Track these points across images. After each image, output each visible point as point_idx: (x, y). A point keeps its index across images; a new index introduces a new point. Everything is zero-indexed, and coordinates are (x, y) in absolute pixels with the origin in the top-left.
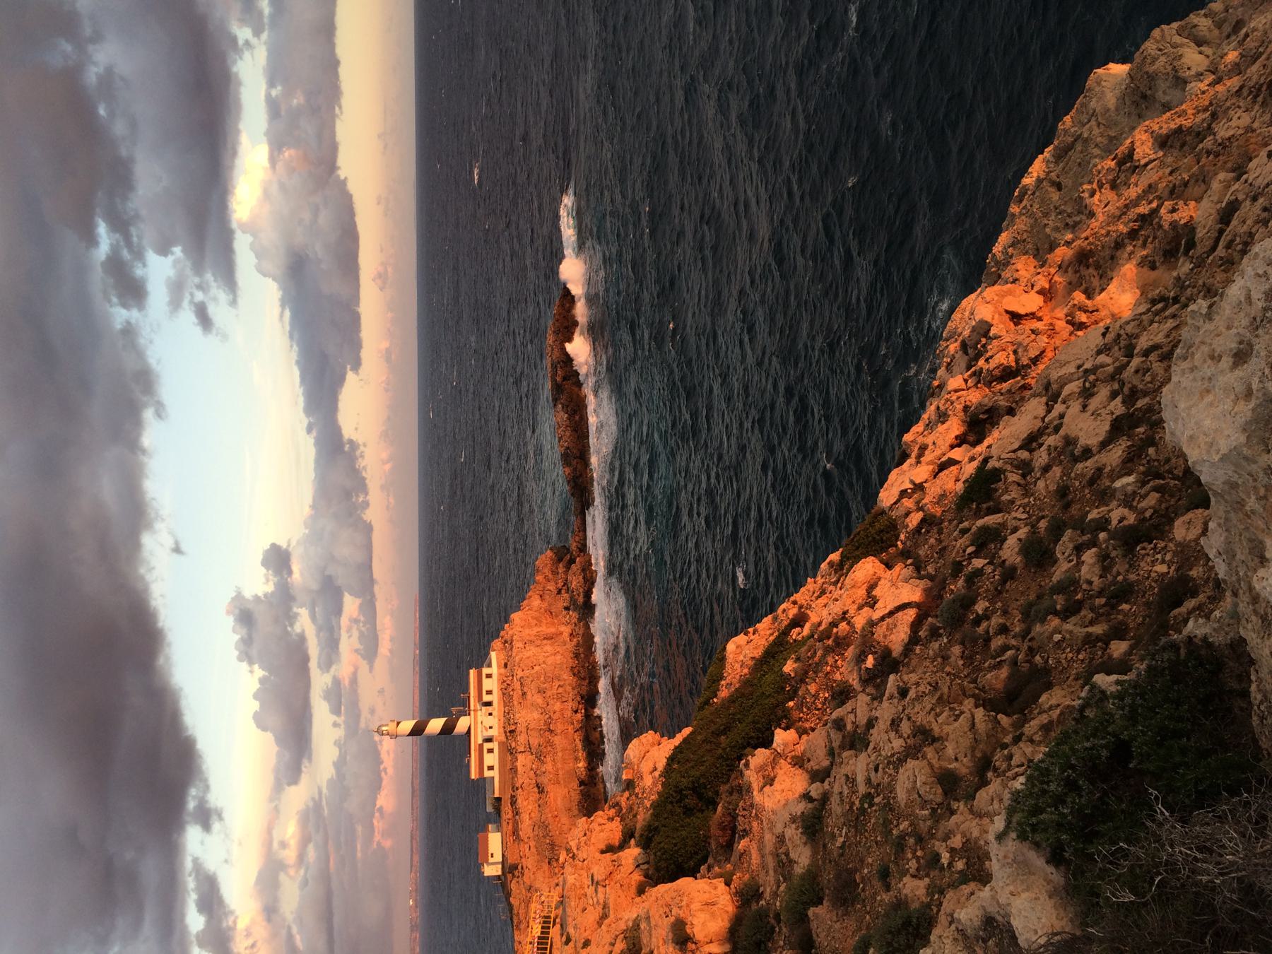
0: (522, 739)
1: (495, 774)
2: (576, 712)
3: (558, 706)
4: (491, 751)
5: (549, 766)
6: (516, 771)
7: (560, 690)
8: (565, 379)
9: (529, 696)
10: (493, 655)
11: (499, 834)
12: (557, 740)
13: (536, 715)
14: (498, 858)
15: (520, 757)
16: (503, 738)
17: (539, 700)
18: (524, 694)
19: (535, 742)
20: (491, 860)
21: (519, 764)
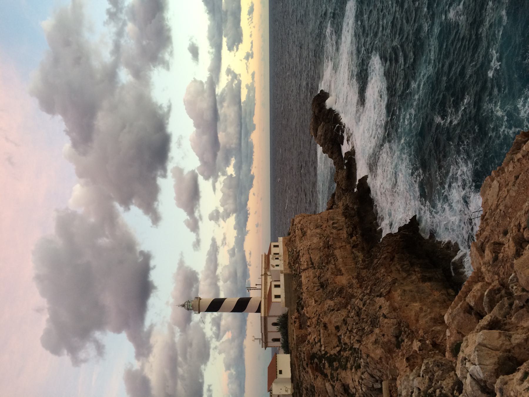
0: (304, 260)
1: (282, 299)
2: (351, 238)
3: (334, 231)
4: (277, 286)
5: (331, 266)
6: (300, 285)
7: (335, 225)
8: (320, 111)
9: (309, 232)
10: (281, 239)
11: (288, 356)
12: (337, 252)
13: (315, 240)
14: (287, 374)
15: (303, 275)
16: (288, 271)
17: (318, 231)
18: (304, 234)
19: (316, 258)
20: (279, 376)
21: (304, 280)
